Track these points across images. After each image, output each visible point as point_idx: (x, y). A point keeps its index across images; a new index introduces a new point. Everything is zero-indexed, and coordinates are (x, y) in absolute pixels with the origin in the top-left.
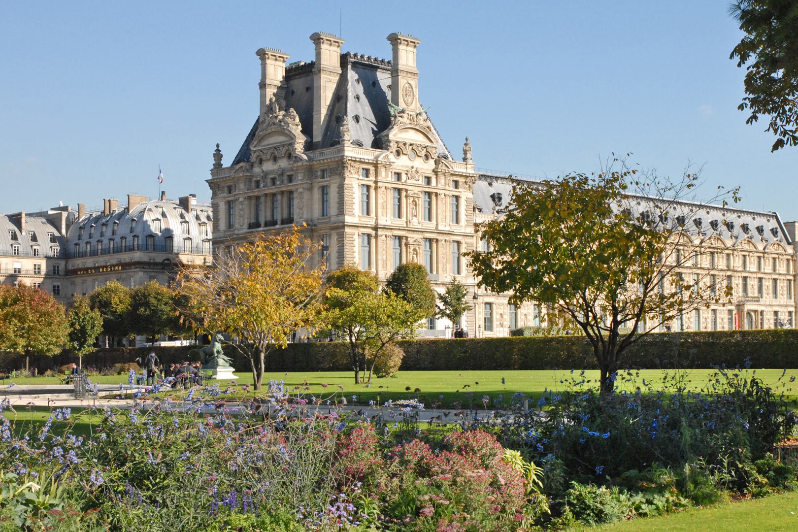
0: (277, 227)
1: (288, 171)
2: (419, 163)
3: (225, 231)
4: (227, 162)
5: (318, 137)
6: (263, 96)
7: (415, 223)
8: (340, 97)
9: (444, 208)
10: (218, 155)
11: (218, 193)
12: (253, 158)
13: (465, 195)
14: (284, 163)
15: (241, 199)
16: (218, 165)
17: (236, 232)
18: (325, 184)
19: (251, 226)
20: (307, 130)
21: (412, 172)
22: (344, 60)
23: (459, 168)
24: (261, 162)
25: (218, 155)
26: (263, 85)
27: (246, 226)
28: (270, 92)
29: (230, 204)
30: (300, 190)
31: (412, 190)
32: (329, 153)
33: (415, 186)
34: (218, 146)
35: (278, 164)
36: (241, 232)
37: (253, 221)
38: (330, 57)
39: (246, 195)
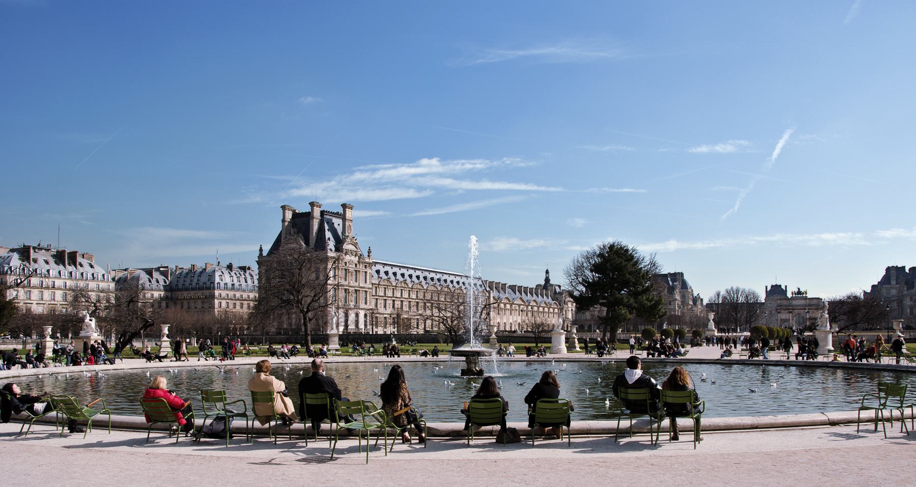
2: (353, 258)
4: (265, 254)
6: (283, 226)
7: (352, 284)
8: (321, 229)
9: (361, 277)
10: (261, 250)
13: (369, 271)
16: (261, 254)
20: (307, 243)
21: (350, 262)
22: (322, 213)
23: (367, 260)
25: (261, 250)
26: (283, 221)
28: (286, 224)
31: (351, 269)
32: (320, 254)
33: (352, 268)
38: (317, 213)
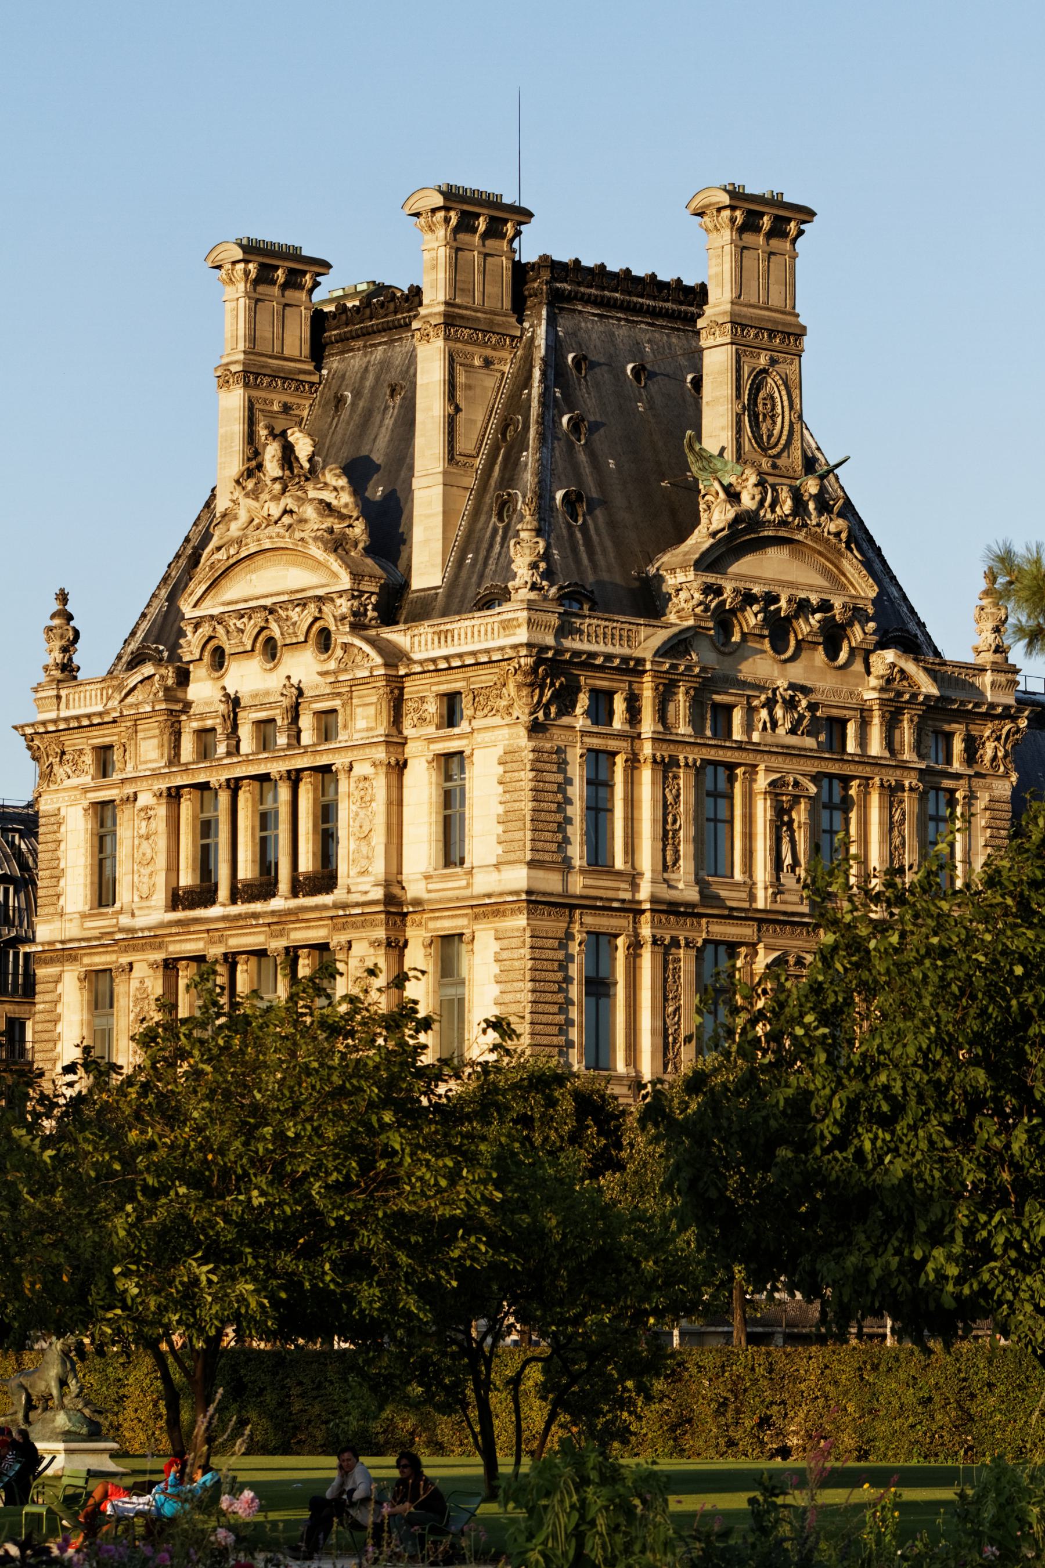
0: (277, 903)
1: (319, 697)
3: (84, 916)
5: (427, 568)
11: (59, 771)
12: (191, 645)
14: (303, 666)
15: (145, 799)
17: (125, 921)
18: (453, 746)
19: (177, 899)
24: (219, 659)
27: (160, 898)
29: (103, 813)
30: (360, 769)
34: (63, 597)
35: (283, 671)
36: (140, 922)
37: (187, 879)
39: (163, 785)
